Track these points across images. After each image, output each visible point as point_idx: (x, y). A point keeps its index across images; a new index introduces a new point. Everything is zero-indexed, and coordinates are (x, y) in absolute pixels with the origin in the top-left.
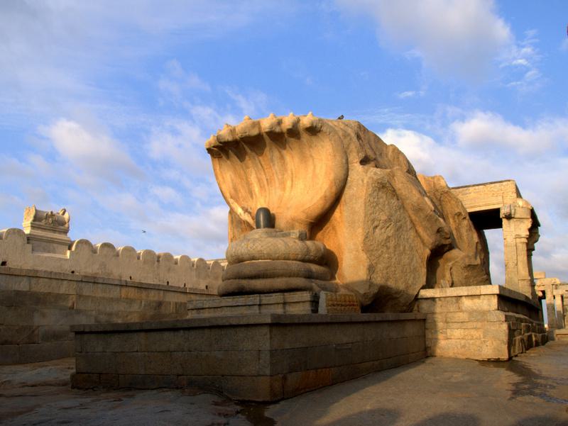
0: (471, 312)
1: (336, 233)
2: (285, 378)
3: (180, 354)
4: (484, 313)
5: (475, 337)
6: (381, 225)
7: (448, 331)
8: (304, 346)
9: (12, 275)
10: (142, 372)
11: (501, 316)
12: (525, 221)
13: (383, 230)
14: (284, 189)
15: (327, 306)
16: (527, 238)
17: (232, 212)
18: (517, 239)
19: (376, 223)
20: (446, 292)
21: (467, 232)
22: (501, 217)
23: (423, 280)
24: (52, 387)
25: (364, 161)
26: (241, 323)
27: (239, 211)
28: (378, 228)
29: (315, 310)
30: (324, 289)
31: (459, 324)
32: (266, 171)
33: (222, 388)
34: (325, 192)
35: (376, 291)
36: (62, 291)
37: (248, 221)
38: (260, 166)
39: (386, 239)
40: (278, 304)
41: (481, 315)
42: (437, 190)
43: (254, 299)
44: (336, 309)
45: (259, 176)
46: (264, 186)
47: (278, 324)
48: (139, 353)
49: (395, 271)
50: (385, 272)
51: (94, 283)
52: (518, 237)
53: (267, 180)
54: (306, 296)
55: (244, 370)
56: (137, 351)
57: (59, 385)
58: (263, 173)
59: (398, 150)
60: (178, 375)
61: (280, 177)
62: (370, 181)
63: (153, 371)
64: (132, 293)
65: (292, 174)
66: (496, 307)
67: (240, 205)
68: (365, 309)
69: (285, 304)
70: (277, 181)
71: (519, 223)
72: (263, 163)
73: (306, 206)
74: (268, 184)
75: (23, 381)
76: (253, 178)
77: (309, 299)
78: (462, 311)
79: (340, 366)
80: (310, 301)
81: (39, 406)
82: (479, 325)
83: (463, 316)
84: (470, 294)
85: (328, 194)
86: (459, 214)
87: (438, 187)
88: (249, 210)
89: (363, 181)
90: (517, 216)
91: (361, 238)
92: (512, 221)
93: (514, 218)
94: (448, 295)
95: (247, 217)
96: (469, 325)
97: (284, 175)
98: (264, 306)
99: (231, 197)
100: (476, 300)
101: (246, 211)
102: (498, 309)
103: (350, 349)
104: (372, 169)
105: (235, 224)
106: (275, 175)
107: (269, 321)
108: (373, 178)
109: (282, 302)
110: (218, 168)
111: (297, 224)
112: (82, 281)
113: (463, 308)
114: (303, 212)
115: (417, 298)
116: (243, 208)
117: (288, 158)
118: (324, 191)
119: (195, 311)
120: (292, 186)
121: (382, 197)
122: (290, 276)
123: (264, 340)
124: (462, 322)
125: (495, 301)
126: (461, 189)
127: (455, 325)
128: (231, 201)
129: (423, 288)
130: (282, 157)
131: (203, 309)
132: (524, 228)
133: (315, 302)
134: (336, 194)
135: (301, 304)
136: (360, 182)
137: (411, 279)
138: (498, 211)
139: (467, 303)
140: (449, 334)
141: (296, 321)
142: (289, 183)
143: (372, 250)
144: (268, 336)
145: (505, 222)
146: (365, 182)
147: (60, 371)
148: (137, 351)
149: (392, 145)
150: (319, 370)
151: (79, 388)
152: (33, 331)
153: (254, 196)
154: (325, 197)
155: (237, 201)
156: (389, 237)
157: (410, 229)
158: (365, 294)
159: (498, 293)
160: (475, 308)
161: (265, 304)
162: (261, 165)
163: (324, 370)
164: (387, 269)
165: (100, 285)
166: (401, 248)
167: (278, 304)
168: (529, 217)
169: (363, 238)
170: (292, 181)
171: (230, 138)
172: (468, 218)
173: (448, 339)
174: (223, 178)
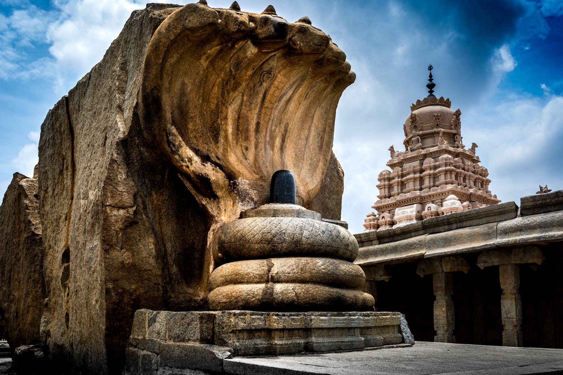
32: (263, 111)
37: (213, 178)
38: (259, 100)
45: (244, 111)
46: (247, 130)
53: (258, 124)
65: (286, 131)
70: (268, 135)
73: (311, 186)
88: (214, 159)
97: (277, 127)
101: (205, 159)
106: (270, 123)
116: (197, 152)
120: (282, 149)
153: (222, 140)
170: (283, 141)
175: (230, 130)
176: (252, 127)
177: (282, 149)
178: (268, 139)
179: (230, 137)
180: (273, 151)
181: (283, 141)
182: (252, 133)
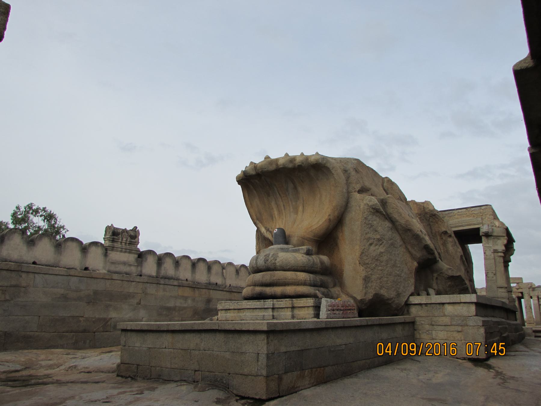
0: (452, 317)
1: (339, 249)
2: (280, 379)
3: (197, 352)
4: (466, 318)
5: (456, 339)
6: (375, 242)
7: (434, 332)
8: (300, 349)
9: (92, 278)
10: (169, 365)
11: (479, 320)
12: (502, 238)
13: (377, 247)
14: (296, 213)
15: (326, 311)
16: (504, 253)
17: (258, 231)
18: (496, 254)
19: (370, 242)
20: (431, 299)
21: (452, 246)
22: (481, 234)
23: (412, 289)
24: (102, 374)
25: (363, 190)
26: (244, 329)
27: (263, 230)
28: (373, 245)
29: (317, 315)
30: (327, 296)
31: (443, 327)
33: (228, 385)
34: (329, 215)
35: (371, 298)
36: (131, 290)
38: (278, 195)
39: (380, 254)
40: (287, 308)
41: (463, 322)
42: (426, 213)
43: (269, 303)
44: (335, 314)
47: (272, 332)
48: (167, 350)
49: (387, 281)
50: (379, 281)
51: (158, 284)
52: (495, 251)
53: (284, 205)
54: (310, 302)
55: (246, 370)
56: (165, 348)
57: (109, 372)
58: (281, 200)
59: (391, 181)
60: (195, 371)
61: (294, 203)
62: (366, 207)
63: (176, 366)
64: (187, 292)
65: (303, 201)
66: (474, 313)
67: (263, 226)
68: (361, 314)
69: (293, 308)
70: (291, 208)
71: (496, 240)
72: (281, 193)
73: (314, 227)
74: (285, 209)
75: (87, 366)
76: (273, 204)
77: (312, 305)
78: (445, 316)
79: (334, 365)
80: (313, 306)
81: (72, 397)
82: (460, 329)
83: (446, 320)
84: (452, 302)
85: (331, 217)
86: (445, 233)
87: (427, 210)
88: (270, 230)
89: (360, 207)
90: (495, 234)
91: (358, 254)
92: (490, 238)
93: (491, 236)
94: (433, 302)
95: (268, 235)
96: (452, 328)
98: (276, 310)
99: (258, 219)
100: (457, 307)
101: (268, 230)
102: (476, 315)
103: (343, 350)
104: (367, 197)
105: (260, 240)
106: (290, 202)
107: (265, 328)
108: (368, 205)
109: (291, 306)
110: (247, 196)
111: (306, 241)
112: (147, 283)
113: (446, 313)
114: (311, 231)
115: (408, 305)
116: (266, 228)
117: (300, 189)
118: (327, 214)
119: (224, 311)
120: (303, 211)
121: (375, 220)
122: (298, 285)
123: (260, 346)
124: (445, 325)
125: (473, 308)
126: (447, 212)
127: (439, 328)
128: (258, 222)
129: (412, 295)
130: (295, 188)
131: (230, 310)
132: (500, 245)
133: (317, 308)
134: (338, 217)
135: (306, 309)
136: (358, 208)
137: (402, 287)
138: (478, 229)
139: (449, 308)
140: (434, 336)
141: (292, 328)
142: (301, 208)
143: (368, 264)
144: (266, 341)
145: (484, 239)
146: (362, 207)
147: (110, 359)
148: (165, 348)
149: (386, 178)
150: (314, 370)
151: (122, 376)
152: (107, 322)
154: (330, 220)
155: (261, 223)
156: (382, 253)
157: (401, 246)
158: (361, 300)
159: (476, 301)
160: (456, 314)
161: (278, 308)
162: (280, 195)
163: (318, 369)
164: (380, 279)
165: (161, 286)
166: (393, 262)
167: (287, 308)
168: (505, 235)
169: (360, 253)
170: (304, 207)
171: (253, 173)
172: (453, 235)
173: (433, 339)
174: (251, 204)
175: (276, 212)
176: (283, 208)
177: (303, 211)
178: (292, 210)
179: (277, 216)
180: (297, 214)
181: (304, 207)
182: (283, 211)
